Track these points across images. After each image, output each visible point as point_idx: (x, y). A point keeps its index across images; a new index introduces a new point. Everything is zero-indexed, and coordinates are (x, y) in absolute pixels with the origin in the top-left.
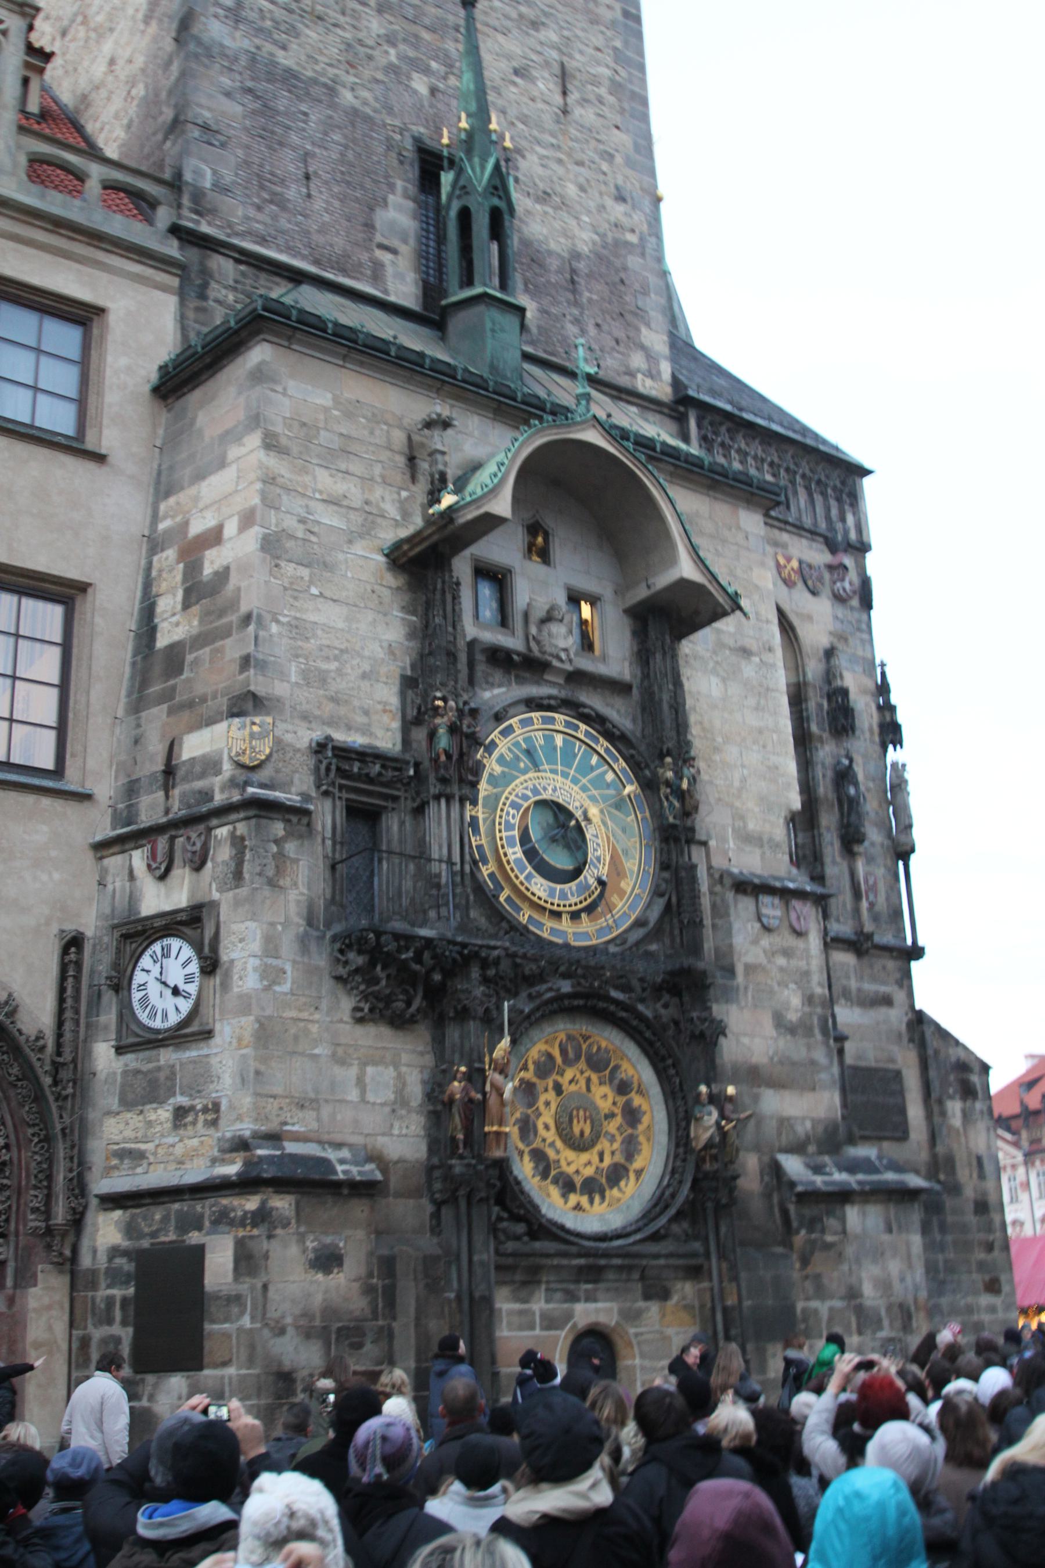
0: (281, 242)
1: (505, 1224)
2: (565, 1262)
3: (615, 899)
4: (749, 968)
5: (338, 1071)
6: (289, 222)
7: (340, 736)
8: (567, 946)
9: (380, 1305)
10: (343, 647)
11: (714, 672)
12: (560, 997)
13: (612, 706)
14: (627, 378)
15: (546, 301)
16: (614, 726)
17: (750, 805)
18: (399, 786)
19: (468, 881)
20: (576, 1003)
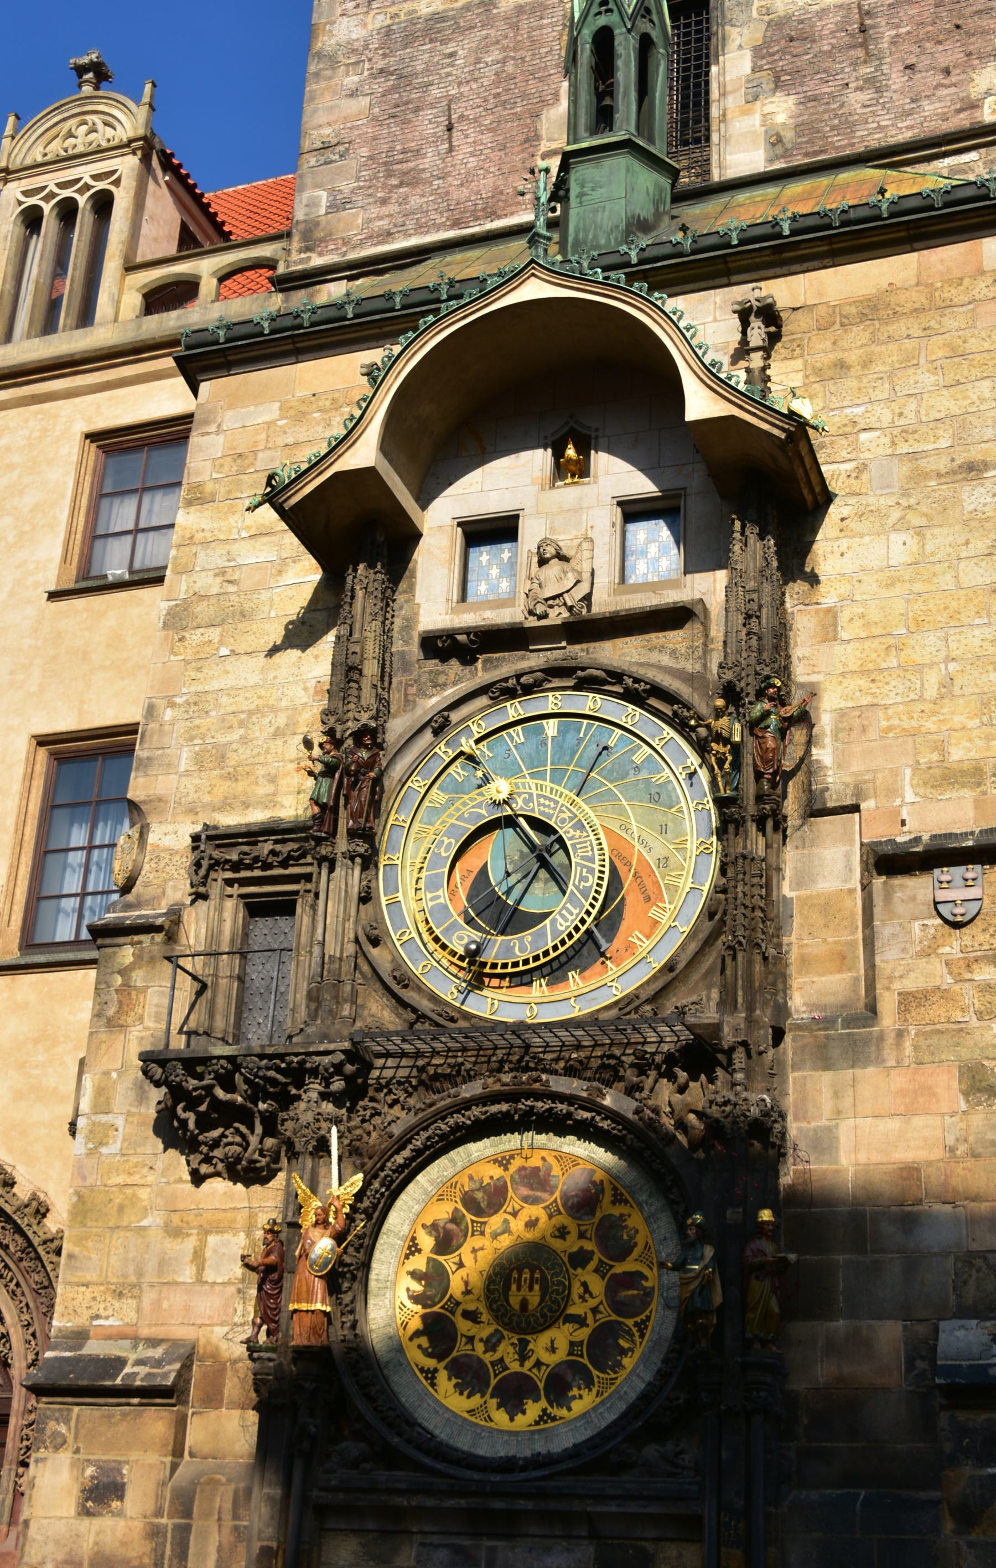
0: (410, 224)
1: (344, 1444)
2: (430, 1502)
3: (636, 937)
4: (908, 1001)
5: (172, 1246)
6: (422, 196)
7: (229, 820)
8: (519, 1028)
9: (168, 1552)
10: (253, 707)
11: (901, 525)
12: (467, 1104)
13: (661, 649)
14: (962, 116)
15: (811, 86)
16: (637, 681)
17: (958, 720)
18: (309, 859)
19: (347, 967)
20: (494, 1109)
